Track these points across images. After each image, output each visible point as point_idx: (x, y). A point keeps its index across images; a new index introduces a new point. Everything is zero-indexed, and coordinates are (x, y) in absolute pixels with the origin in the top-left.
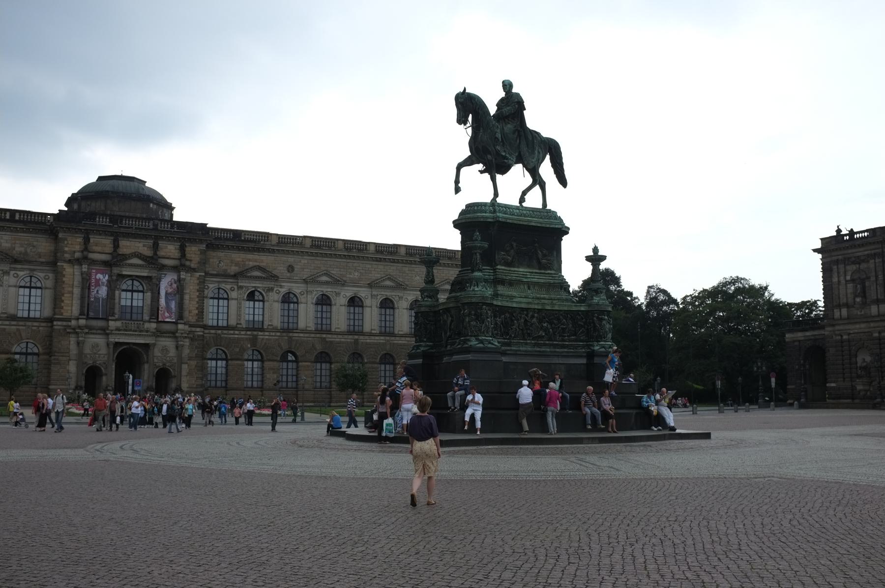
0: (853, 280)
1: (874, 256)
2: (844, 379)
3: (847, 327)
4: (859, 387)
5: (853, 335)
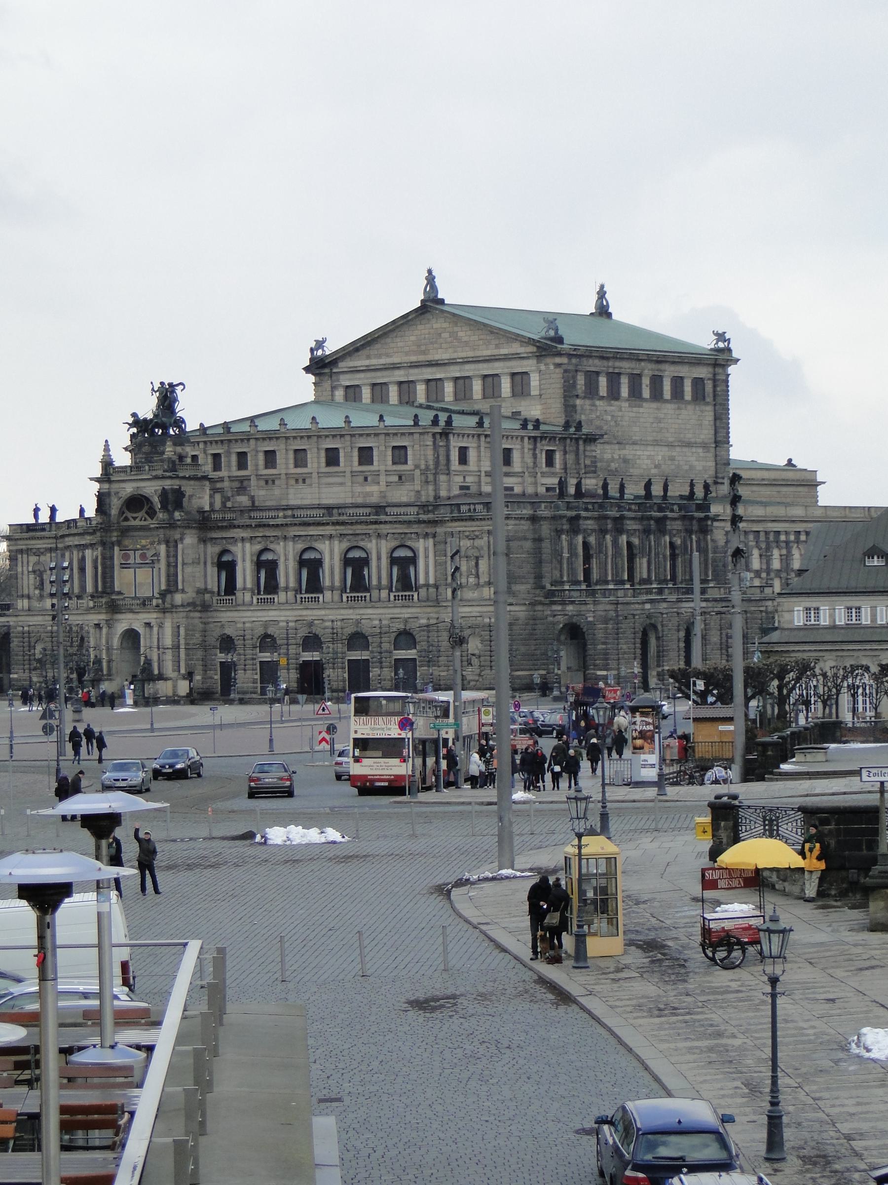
0: (34, 572)
1: (50, 550)
3: (28, 618)
4: (35, 679)
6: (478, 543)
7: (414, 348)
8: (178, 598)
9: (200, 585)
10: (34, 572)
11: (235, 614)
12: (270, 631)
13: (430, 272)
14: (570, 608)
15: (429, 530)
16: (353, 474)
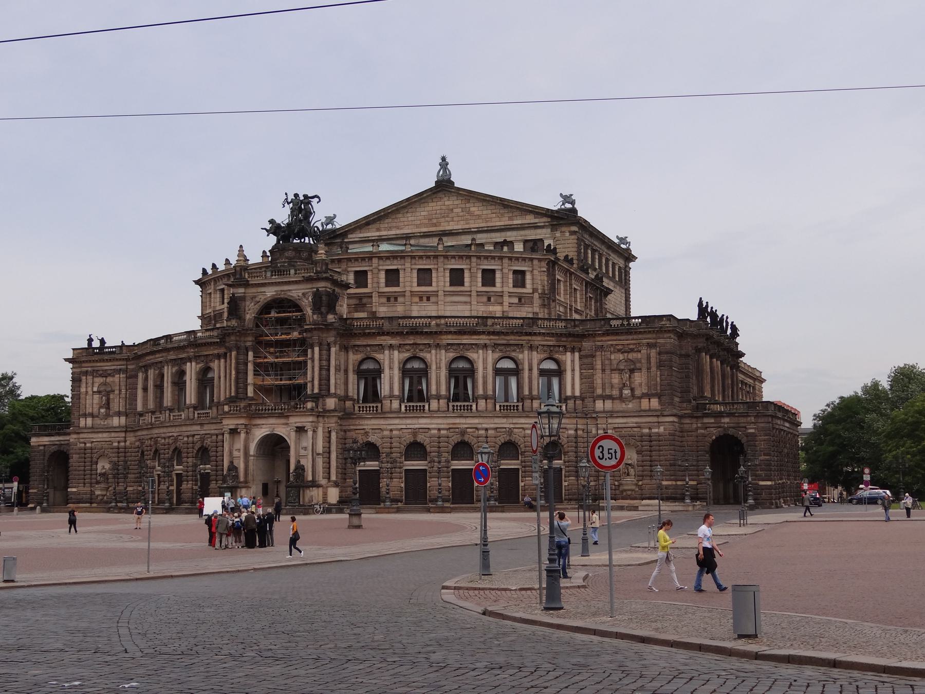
0: (99, 392)
1: (119, 371)
2: (84, 484)
5: (96, 443)
6: (631, 356)
7: (426, 221)
8: (331, 403)
9: (341, 392)
10: (99, 392)
11: (382, 422)
12: (420, 438)
13: (444, 159)
14: (726, 420)
15: (577, 345)
16: (479, 294)
